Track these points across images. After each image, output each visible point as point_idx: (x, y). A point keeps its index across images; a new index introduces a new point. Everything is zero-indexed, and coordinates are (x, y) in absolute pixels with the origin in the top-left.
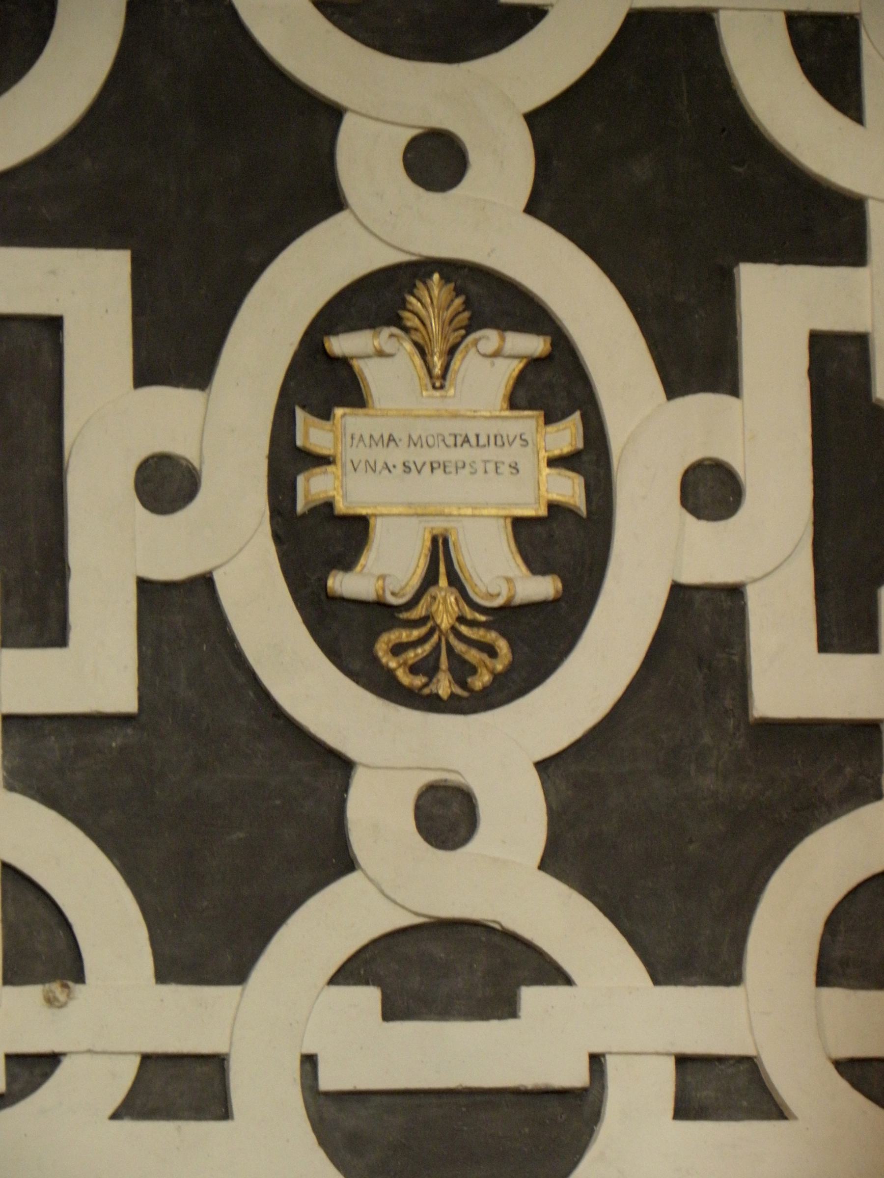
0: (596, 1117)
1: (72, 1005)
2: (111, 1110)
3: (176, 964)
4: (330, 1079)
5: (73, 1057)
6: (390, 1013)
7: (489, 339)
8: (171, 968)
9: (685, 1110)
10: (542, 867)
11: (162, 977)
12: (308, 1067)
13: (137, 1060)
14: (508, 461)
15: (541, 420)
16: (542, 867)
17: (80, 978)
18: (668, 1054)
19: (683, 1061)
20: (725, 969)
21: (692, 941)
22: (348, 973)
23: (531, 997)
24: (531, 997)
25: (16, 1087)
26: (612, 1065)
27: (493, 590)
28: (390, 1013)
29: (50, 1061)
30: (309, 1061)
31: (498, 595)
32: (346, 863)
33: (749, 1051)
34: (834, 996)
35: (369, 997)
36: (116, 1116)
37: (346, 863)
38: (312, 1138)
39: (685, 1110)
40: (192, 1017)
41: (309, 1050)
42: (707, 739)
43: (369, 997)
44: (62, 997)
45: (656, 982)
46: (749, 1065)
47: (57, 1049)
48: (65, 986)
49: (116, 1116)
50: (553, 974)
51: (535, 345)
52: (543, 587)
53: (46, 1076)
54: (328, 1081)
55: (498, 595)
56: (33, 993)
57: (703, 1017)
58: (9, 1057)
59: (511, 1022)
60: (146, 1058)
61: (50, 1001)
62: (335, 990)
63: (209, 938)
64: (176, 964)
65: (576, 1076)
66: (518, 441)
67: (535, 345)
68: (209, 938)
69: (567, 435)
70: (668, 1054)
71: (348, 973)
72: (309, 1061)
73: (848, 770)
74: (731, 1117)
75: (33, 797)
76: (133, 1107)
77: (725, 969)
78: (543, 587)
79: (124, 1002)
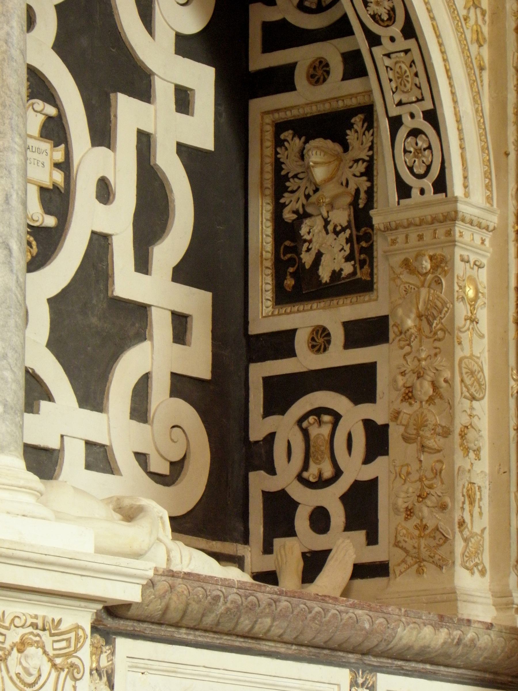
7: (39, 104)
14: (41, 161)
15: (53, 146)
18: (83, 440)
23: (44, 404)
27: (35, 218)
31: (37, 221)
33: (106, 442)
42: (94, 302)
51: (52, 111)
52: (50, 221)
55: (37, 221)
57: (92, 425)
66: (45, 153)
67: (52, 111)
69: (59, 155)
70: (83, 440)
73: (137, 325)
78: (50, 221)
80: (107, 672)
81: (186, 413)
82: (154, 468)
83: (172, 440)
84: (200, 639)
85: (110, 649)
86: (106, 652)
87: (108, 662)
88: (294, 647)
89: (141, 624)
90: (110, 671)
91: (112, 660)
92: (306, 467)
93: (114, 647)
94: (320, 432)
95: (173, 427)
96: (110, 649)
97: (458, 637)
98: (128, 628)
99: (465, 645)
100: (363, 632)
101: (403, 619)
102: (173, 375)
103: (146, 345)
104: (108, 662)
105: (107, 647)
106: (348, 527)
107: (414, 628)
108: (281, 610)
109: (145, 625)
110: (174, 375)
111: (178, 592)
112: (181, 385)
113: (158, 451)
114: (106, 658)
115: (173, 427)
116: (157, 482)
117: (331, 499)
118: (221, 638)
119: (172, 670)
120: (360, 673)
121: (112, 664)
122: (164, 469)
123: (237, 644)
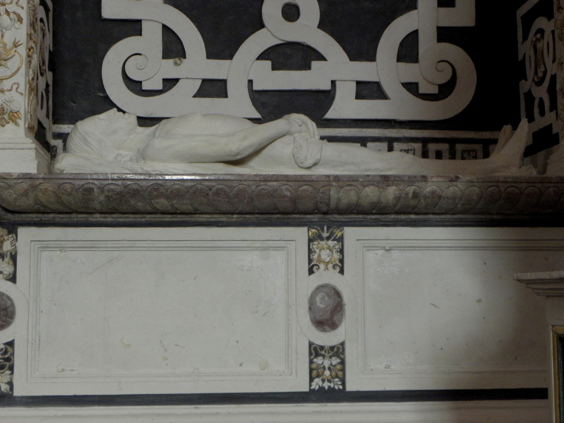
0: (333, 98)
1: (182, 65)
2: (193, 95)
4: (257, 87)
6: (274, 68)
8: (211, 55)
9: (359, 96)
10: (319, 27)
12: (250, 83)
13: (201, 81)
16: (319, 27)
17: (184, 57)
18: (354, 81)
19: (358, 83)
20: (372, 58)
21: (361, 49)
22: (262, 57)
23: (315, 64)
24: (315, 64)
25: (166, 88)
26: (338, 83)
28: (274, 68)
30: (250, 82)
32: (262, 26)
33: (376, 80)
34: (402, 65)
35: (268, 64)
36: (194, 96)
37: (262, 26)
38: (251, 103)
39: (359, 96)
40: (217, 69)
43: (268, 64)
44: (178, 62)
45: (351, 60)
46: (377, 84)
47: (178, 77)
48: (180, 59)
49: (194, 96)
50: (321, 58)
53: (175, 85)
54: (256, 87)
56: (171, 62)
57: (365, 71)
58: (164, 80)
59: (309, 71)
60: (204, 81)
61: (176, 64)
62: (258, 61)
63: (222, 45)
65: (327, 86)
68: (222, 45)
70: (354, 81)
71: (262, 57)
72: (250, 82)
74: (371, 99)
75: (172, 6)
76: (200, 94)
77: (372, 58)
80: (11, 254)
81: (454, 53)
82: (421, 91)
83: (438, 71)
84: (120, 220)
85: (13, 237)
86: (8, 239)
87: (12, 246)
88: (235, 216)
89: (46, 215)
90: (14, 253)
91: (15, 245)
92: (536, 73)
93: (17, 236)
94: (539, 45)
95: (439, 62)
96: (13, 237)
97: (412, 191)
98: (35, 219)
99: (426, 197)
100: (286, 199)
101: (334, 184)
102: (438, 28)
103: (413, 13)
104: (12, 246)
105: (11, 236)
106: (551, 110)
107: (350, 190)
108: (172, 192)
109: (51, 216)
110: (439, 29)
111: (41, 190)
112: (445, 34)
113: (426, 79)
114: (10, 245)
115: (439, 62)
116: (424, 99)
117: (541, 92)
118: (145, 217)
119: (92, 246)
120: (325, 228)
121: (16, 248)
122: (435, 90)
123: (167, 219)
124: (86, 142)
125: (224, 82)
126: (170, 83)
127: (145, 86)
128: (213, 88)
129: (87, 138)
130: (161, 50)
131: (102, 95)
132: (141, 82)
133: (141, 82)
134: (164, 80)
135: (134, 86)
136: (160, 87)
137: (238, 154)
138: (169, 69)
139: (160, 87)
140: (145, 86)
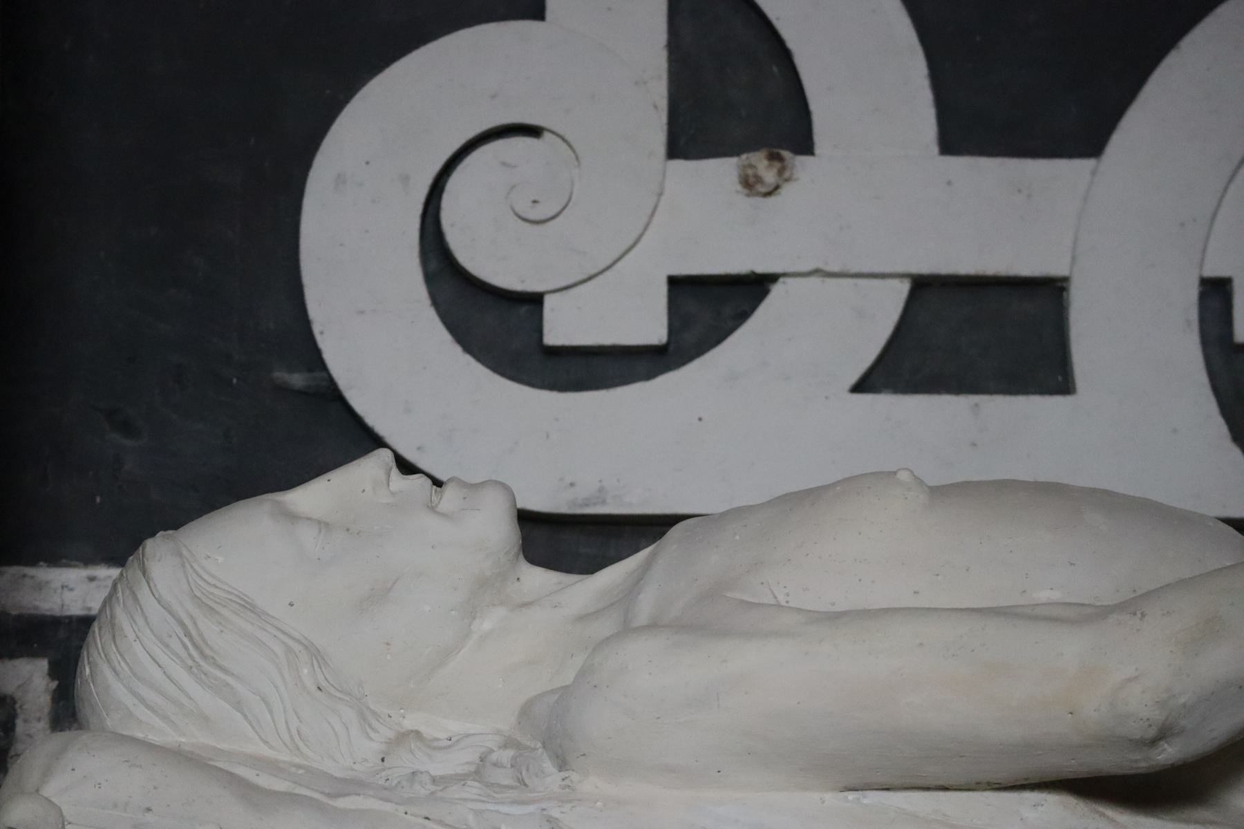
1: (786, 189)
2: (854, 378)
3: (977, 119)
5: (789, 280)
11: (950, 143)
13: (904, 288)
17: (805, 146)
29: (749, 290)
30: (1216, 294)
36: (861, 387)
40: (1002, 215)
41: (1211, 271)
44: (769, 176)
47: (761, 268)
48: (774, 157)
49: (861, 387)
53: (743, 316)
56: (720, 172)
58: (675, 283)
60: (922, 286)
61: (749, 183)
64: (977, 119)
72: (1216, 294)
76: (892, 372)
79: (885, 191)
124: (200, 655)
125: (1049, 293)
126: (712, 306)
127: (564, 326)
128: (979, 336)
129: (208, 627)
130: (663, 103)
131: (297, 380)
132: (536, 300)
133: (536, 300)
134: (675, 283)
135: (496, 325)
136: (649, 325)
137: (1164, 734)
138: (710, 215)
139: (649, 325)
140: (564, 326)
